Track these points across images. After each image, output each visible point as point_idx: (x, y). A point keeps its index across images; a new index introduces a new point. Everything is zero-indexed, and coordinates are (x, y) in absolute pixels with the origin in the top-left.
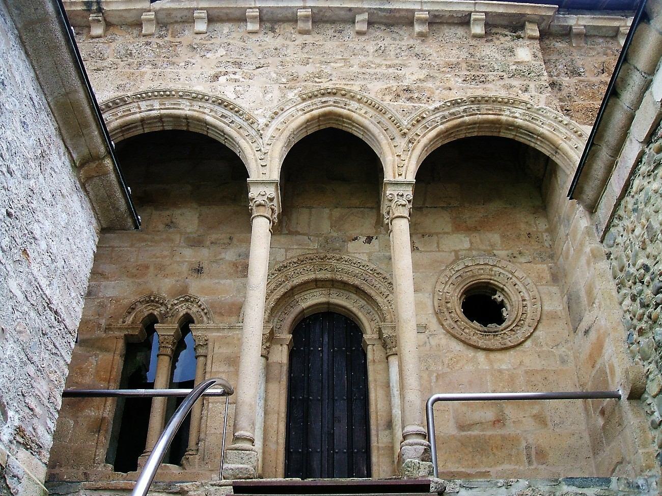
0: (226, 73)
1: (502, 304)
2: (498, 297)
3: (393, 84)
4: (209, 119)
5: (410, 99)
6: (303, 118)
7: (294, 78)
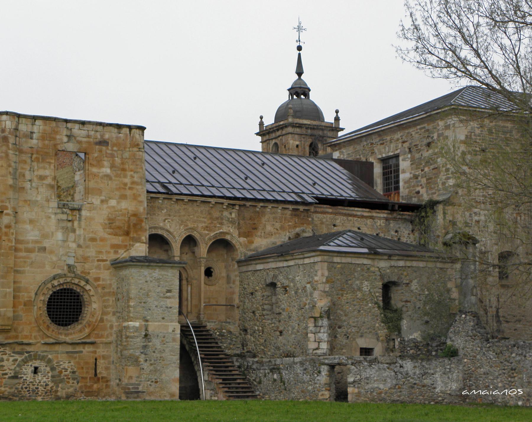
0: (167, 219)
1: (212, 272)
2: (212, 270)
3: (204, 225)
4: (165, 235)
5: (207, 230)
6: (185, 236)
7: (182, 221)
